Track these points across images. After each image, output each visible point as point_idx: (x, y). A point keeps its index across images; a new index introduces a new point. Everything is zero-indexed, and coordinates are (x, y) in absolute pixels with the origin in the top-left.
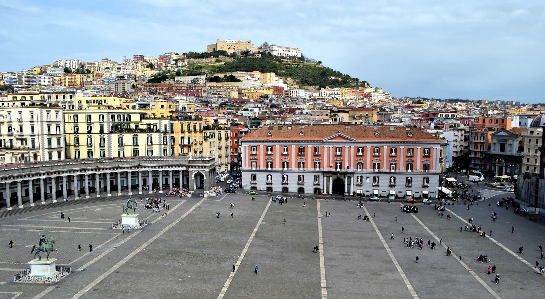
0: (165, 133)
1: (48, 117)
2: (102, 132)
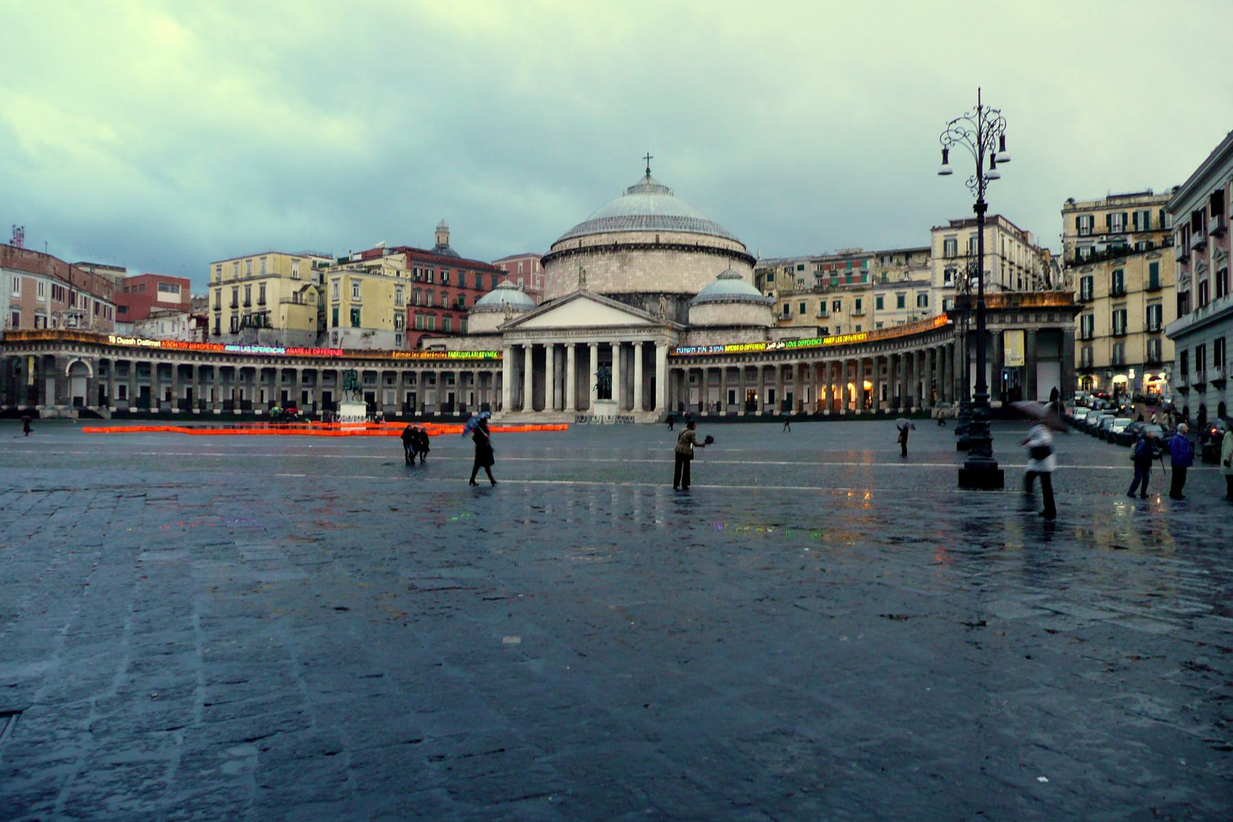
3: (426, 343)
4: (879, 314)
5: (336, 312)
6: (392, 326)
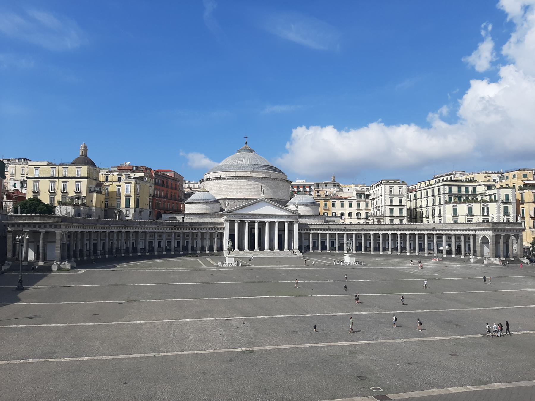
0: (506, 202)
1: (391, 191)
2: (440, 204)
3: (165, 217)
4: (334, 209)
5: (128, 200)
6: (148, 208)
